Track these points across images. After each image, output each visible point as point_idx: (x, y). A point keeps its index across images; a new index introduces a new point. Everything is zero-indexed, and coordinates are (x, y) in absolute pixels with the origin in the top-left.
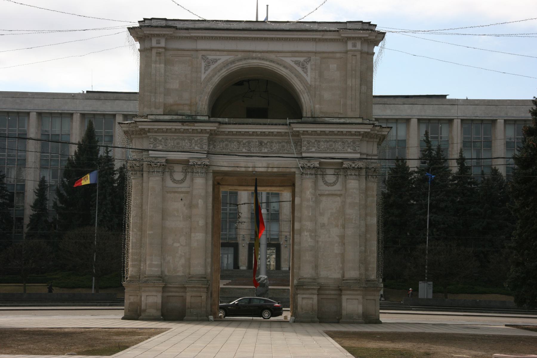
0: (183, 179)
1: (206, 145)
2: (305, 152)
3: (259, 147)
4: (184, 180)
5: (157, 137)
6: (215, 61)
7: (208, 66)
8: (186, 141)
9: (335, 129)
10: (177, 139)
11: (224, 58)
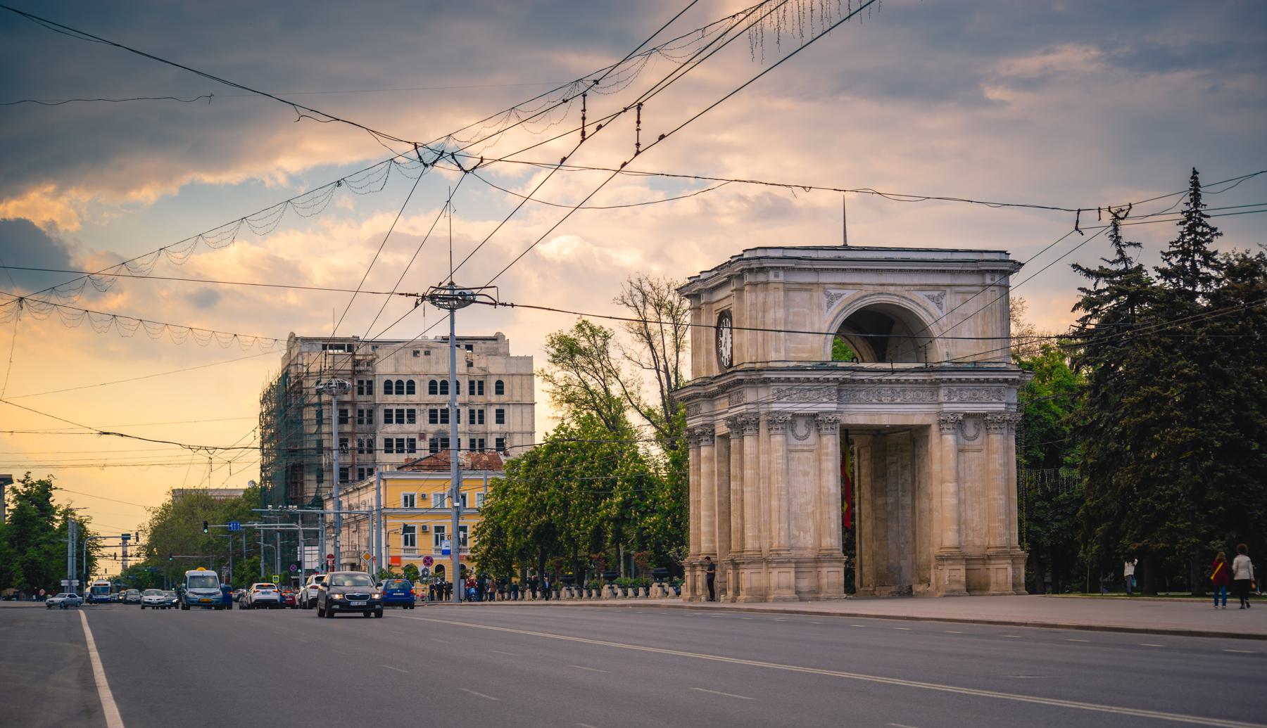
6: (841, 296)
7: (830, 304)
9: (992, 376)
11: (849, 294)
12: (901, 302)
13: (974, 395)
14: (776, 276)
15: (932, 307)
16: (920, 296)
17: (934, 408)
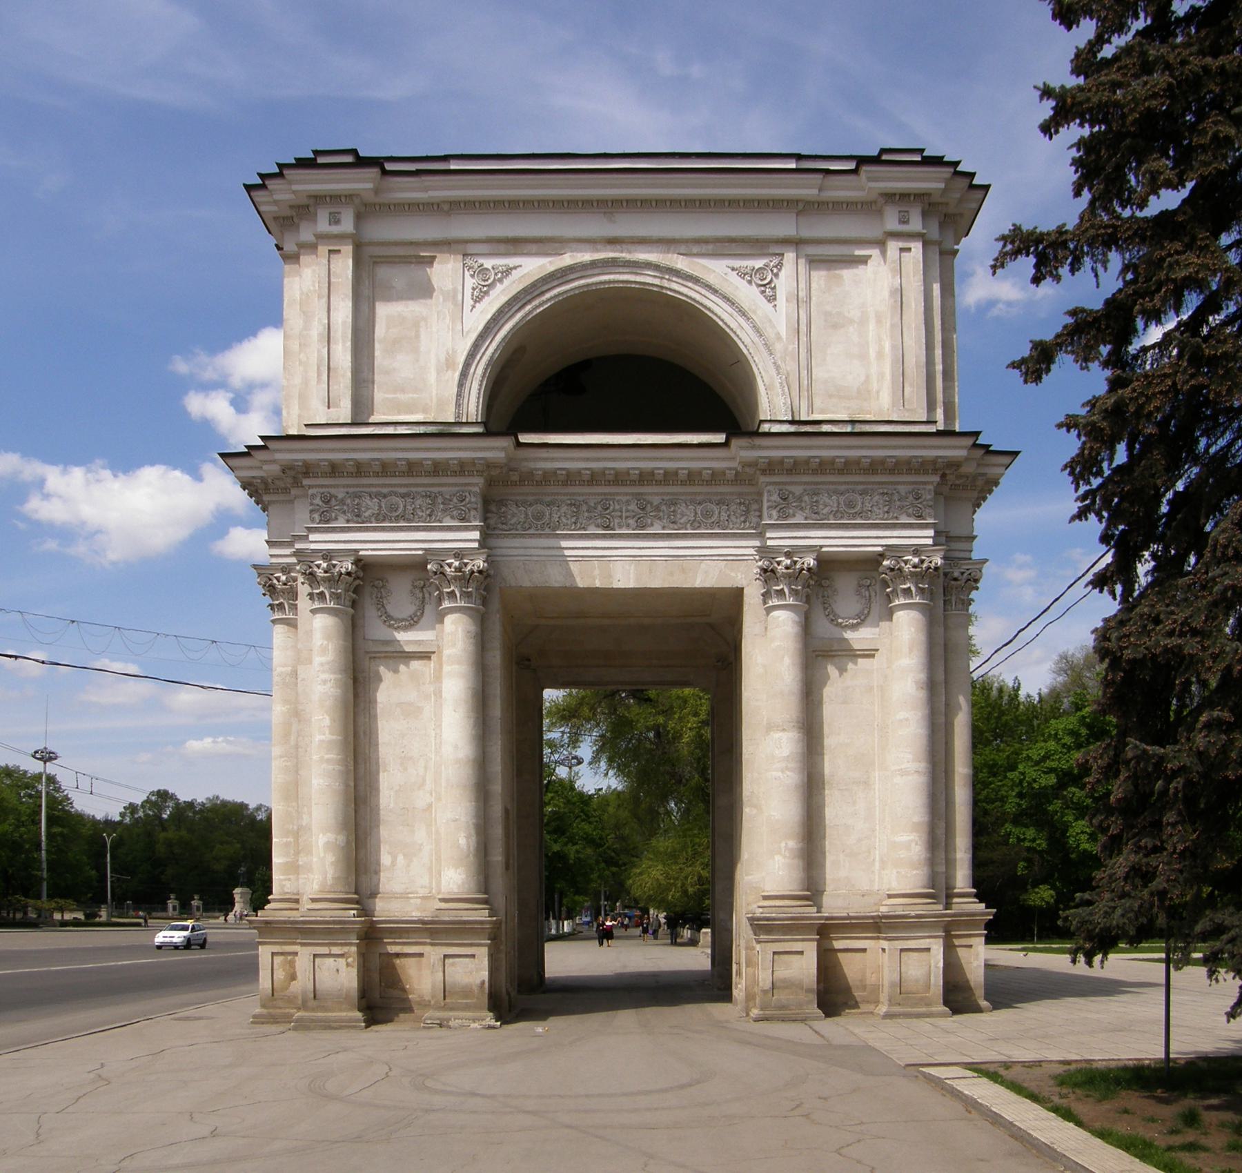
1: (476, 509)
2: (772, 526)
4: (415, 619)
5: (333, 491)
6: (508, 271)
8: (418, 502)
10: (390, 494)
11: (531, 267)
12: (666, 284)
13: (851, 505)
15: (747, 294)
16: (717, 270)
17: (748, 547)
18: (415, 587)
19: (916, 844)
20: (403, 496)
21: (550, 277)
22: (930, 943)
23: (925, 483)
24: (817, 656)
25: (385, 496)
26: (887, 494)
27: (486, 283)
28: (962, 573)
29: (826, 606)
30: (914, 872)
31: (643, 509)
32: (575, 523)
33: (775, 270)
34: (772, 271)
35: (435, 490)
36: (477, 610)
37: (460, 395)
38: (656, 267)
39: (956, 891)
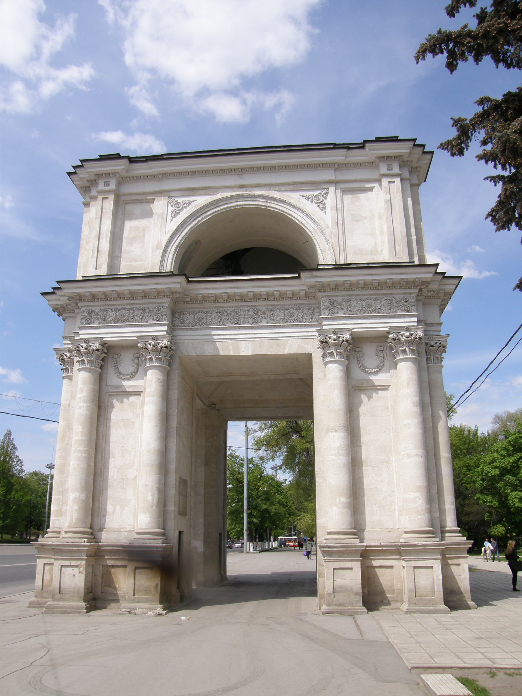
0: (134, 372)
1: (165, 315)
3: (253, 318)
5: (93, 308)
6: (189, 203)
8: (136, 312)
10: (122, 309)
11: (201, 200)
12: (268, 205)
13: (369, 306)
14: (107, 184)
15: (311, 207)
17: (312, 332)
18: (134, 357)
19: (420, 499)
20: (128, 310)
21: (210, 204)
22: (432, 563)
23: (410, 293)
24: (355, 390)
25: (119, 310)
26: (389, 299)
27: (179, 209)
28: (436, 343)
29: (359, 362)
30: (420, 517)
31: (256, 314)
32: (220, 322)
33: (325, 196)
34: (323, 196)
35: (145, 306)
36: (165, 368)
37: (162, 261)
38: (264, 197)
39: (447, 529)
